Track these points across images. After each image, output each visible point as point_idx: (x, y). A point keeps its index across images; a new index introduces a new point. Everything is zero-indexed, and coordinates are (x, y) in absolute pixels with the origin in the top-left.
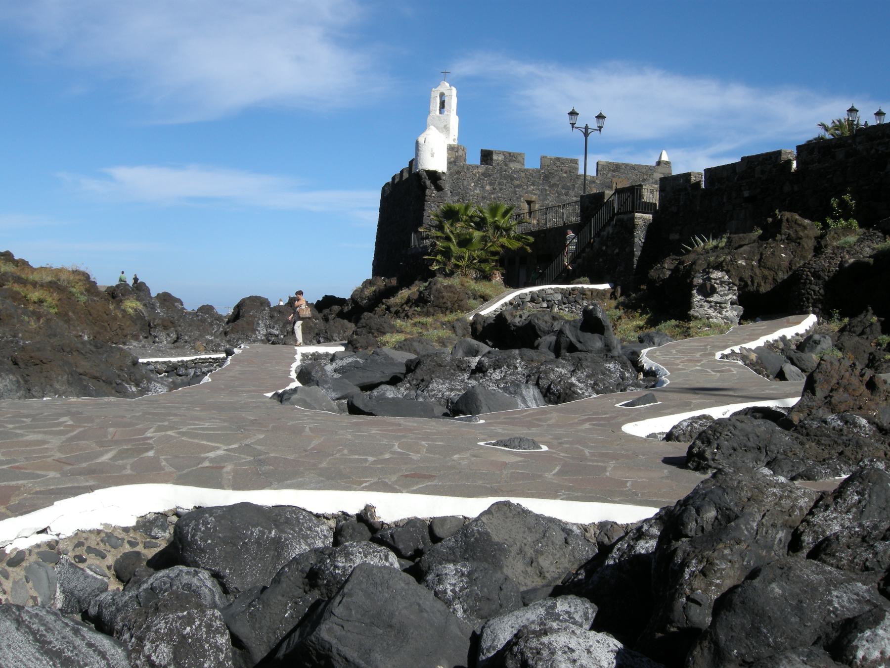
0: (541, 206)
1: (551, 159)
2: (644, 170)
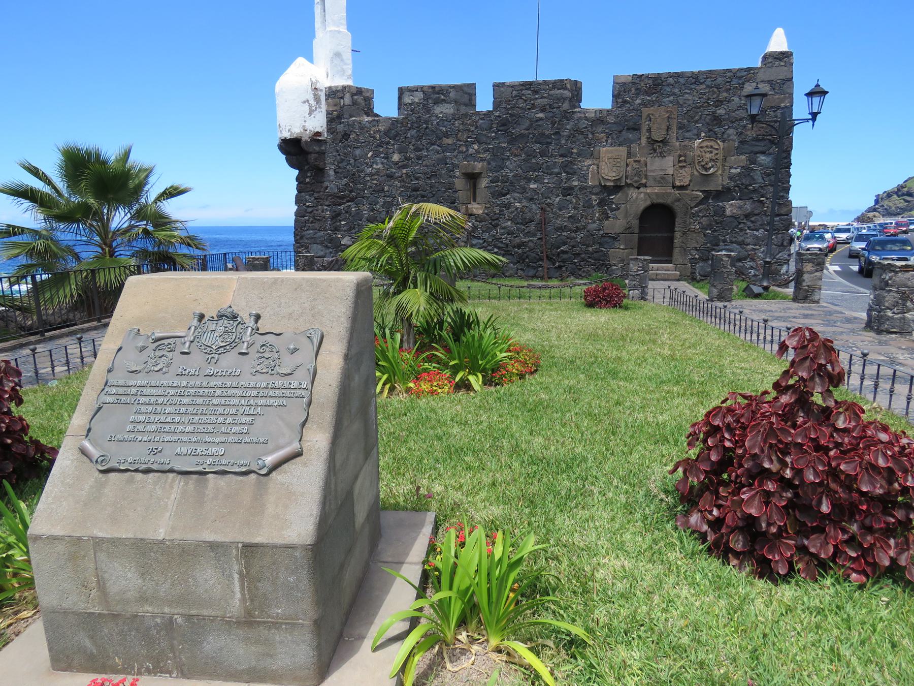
0: (492, 182)
2: (720, 80)
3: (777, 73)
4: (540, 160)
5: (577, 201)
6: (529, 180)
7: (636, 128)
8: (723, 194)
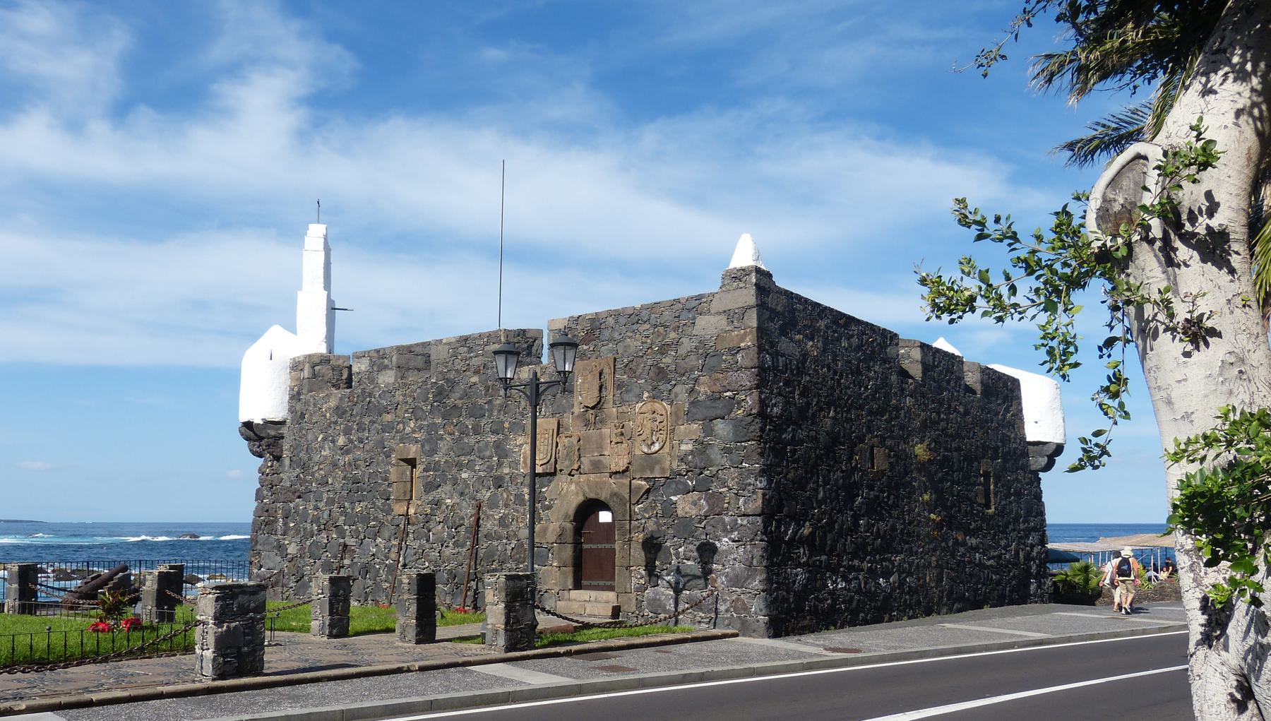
0: (425, 470)
1: (449, 344)
5: (508, 496)
6: (460, 467)
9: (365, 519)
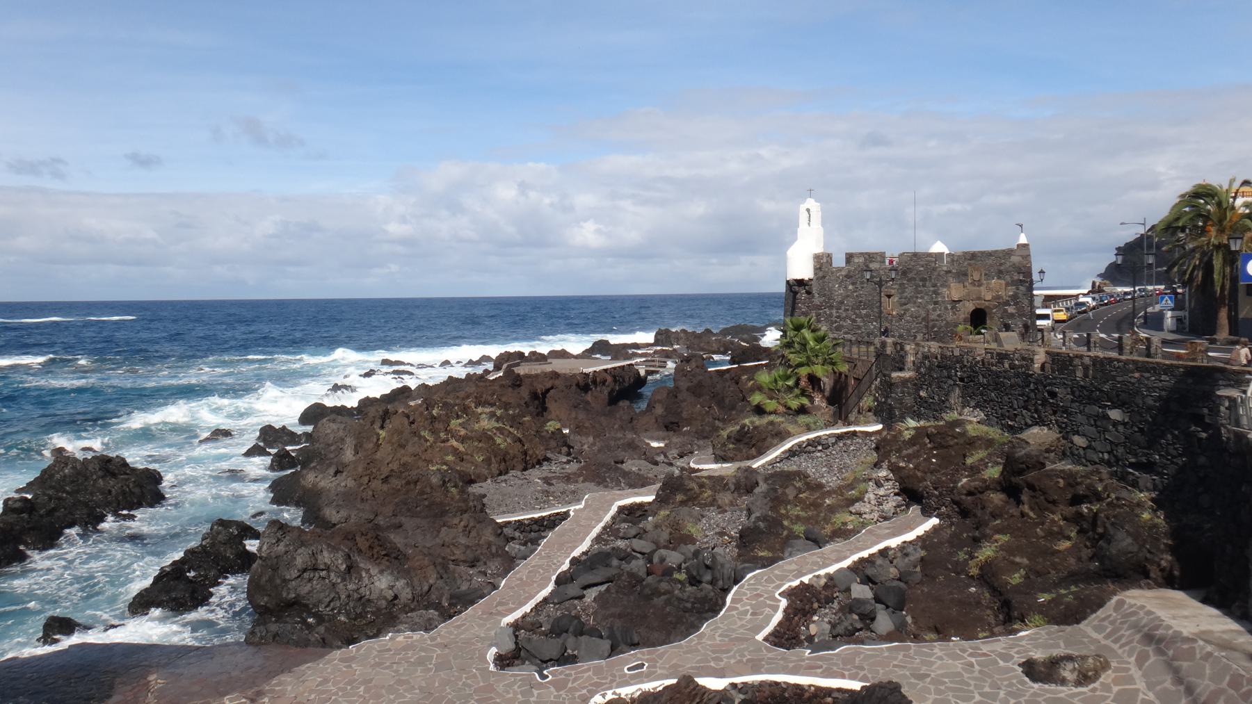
2: (1001, 255)
3: (1024, 253)
4: (921, 289)
6: (917, 298)
7: (965, 275)
8: (1007, 303)
9: (867, 316)
